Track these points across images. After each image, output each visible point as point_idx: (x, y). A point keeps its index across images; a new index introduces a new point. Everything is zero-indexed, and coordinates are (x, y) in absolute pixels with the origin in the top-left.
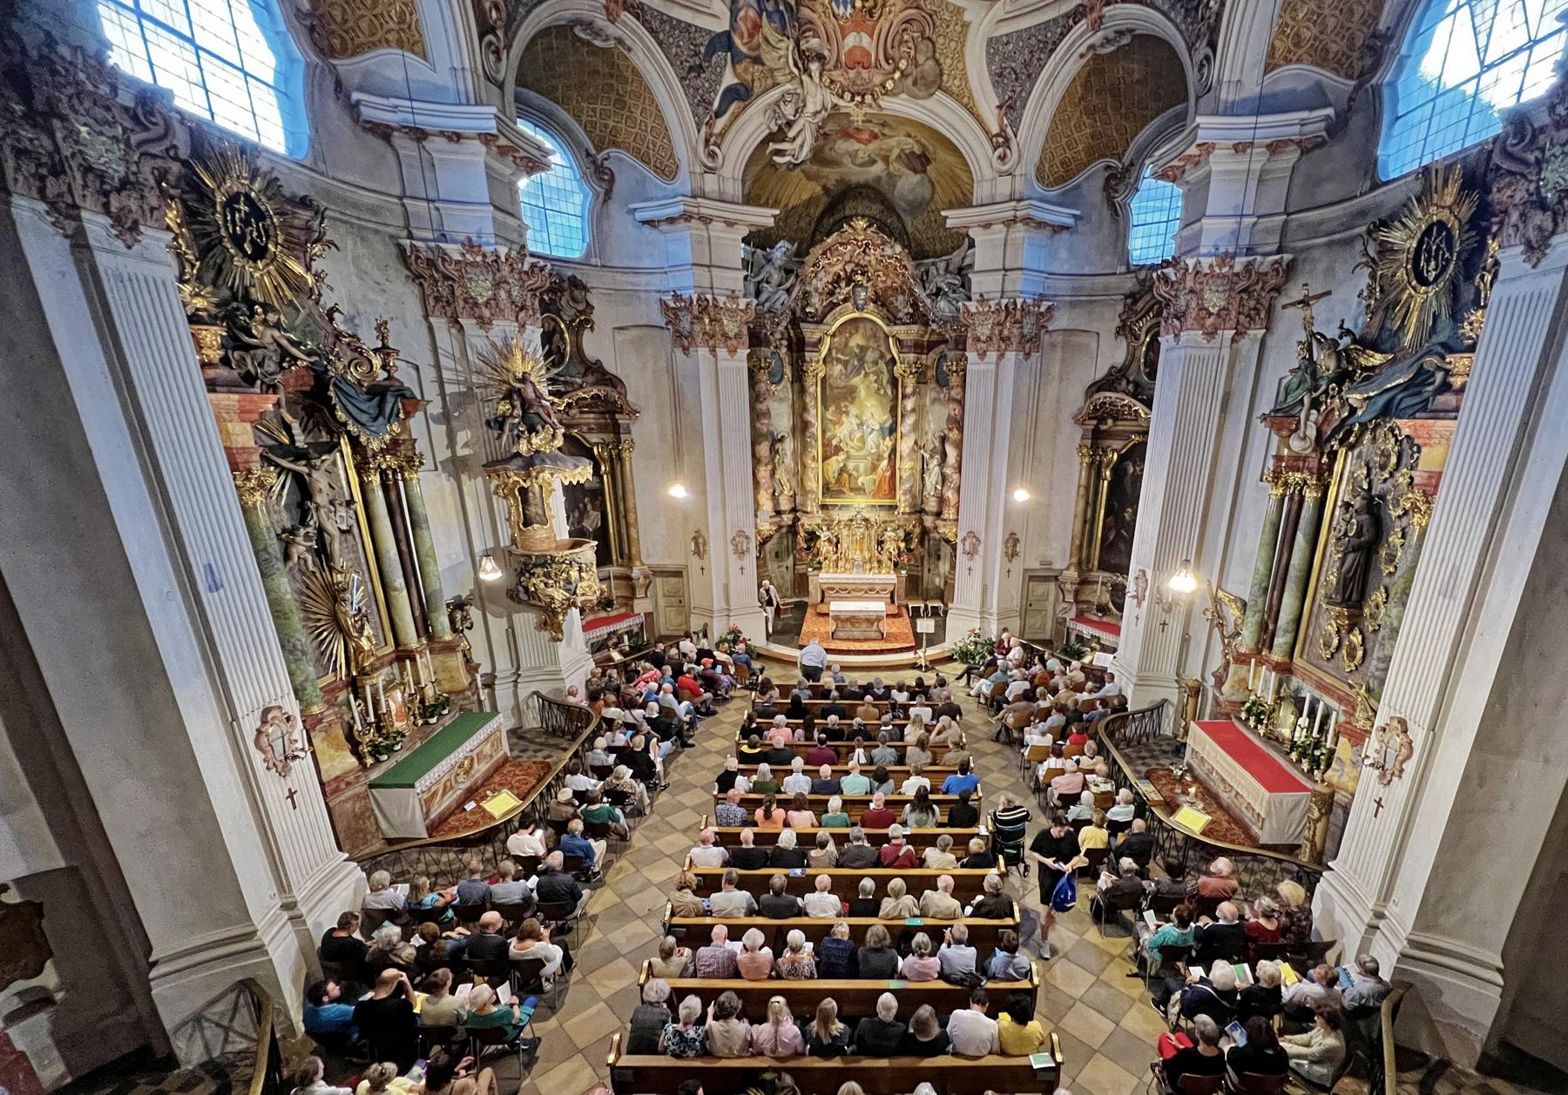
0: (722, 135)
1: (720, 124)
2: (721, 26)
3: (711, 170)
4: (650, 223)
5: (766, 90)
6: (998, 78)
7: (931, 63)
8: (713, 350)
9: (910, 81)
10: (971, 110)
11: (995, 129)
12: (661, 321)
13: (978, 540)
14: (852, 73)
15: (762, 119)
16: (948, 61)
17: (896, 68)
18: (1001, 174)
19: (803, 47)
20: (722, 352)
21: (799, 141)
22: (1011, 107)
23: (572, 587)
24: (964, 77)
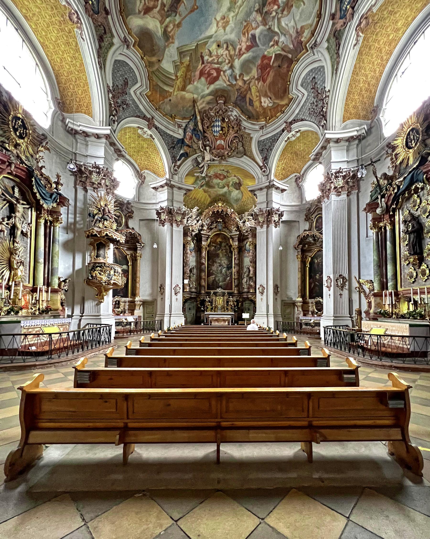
0: (179, 167)
1: (178, 163)
2: (180, 137)
3: (176, 174)
4: (155, 188)
5: (193, 155)
6: (261, 151)
7: (241, 148)
8: (172, 225)
9: (235, 153)
10: (254, 160)
11: (261, 164)
12: (155, 217)
13: (264, 287)
14: (219, 151)
15: (191, 163)
16: (247, 148)
17: (231, 149)
18: (264, 176)
19: (205, 143)
20: (174, 225)
21: (202, 169)
22: (266, 159)
23: (110, 277)
24: (251, 152)
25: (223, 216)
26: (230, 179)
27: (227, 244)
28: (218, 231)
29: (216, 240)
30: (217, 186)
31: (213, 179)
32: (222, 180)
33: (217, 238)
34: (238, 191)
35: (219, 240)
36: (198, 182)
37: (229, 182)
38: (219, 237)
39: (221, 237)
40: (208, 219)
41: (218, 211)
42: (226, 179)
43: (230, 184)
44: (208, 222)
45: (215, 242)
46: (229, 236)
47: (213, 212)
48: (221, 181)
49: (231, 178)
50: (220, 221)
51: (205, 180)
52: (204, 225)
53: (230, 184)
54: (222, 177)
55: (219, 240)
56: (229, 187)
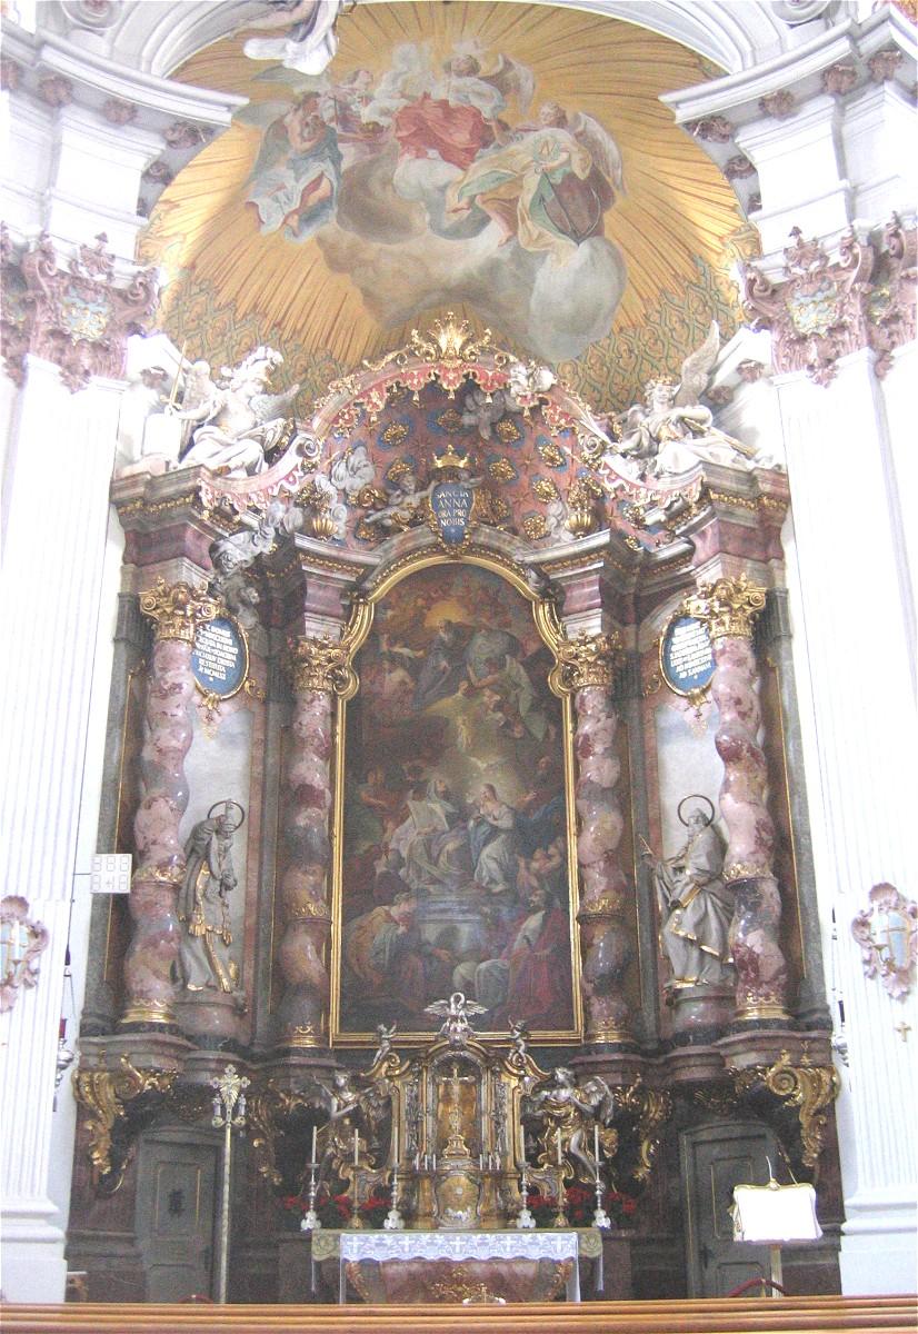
25: (474, 429)
26: (522, 150)
27: (515, 647)
28: (436, 549)
29: (419, 618)
30: (421, 220)
31: (394, 157)
32: (462, 166)
33: (430, 602)
34: (585, 248)
35: (446, 614)
36: (283, 173)
37: (517, 182)
38: (445, 595)
39: (458, 590)
40: (358, 458)
41: (433, 390)
42: (489, 153)
43: (526, 198)
44: (358, 483)
45: (412, 630)
46: (529, 588)
47: (398, 399)
48: (457, 173)
49: (531, 138)
50: (452, 472)
51: (337, 159)
52: (325, 497)
53: (526, 198)
54: (461, 138)
55: (446, 614)
56: (512, 222)
